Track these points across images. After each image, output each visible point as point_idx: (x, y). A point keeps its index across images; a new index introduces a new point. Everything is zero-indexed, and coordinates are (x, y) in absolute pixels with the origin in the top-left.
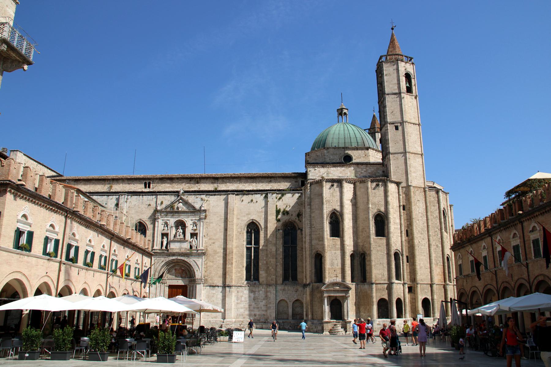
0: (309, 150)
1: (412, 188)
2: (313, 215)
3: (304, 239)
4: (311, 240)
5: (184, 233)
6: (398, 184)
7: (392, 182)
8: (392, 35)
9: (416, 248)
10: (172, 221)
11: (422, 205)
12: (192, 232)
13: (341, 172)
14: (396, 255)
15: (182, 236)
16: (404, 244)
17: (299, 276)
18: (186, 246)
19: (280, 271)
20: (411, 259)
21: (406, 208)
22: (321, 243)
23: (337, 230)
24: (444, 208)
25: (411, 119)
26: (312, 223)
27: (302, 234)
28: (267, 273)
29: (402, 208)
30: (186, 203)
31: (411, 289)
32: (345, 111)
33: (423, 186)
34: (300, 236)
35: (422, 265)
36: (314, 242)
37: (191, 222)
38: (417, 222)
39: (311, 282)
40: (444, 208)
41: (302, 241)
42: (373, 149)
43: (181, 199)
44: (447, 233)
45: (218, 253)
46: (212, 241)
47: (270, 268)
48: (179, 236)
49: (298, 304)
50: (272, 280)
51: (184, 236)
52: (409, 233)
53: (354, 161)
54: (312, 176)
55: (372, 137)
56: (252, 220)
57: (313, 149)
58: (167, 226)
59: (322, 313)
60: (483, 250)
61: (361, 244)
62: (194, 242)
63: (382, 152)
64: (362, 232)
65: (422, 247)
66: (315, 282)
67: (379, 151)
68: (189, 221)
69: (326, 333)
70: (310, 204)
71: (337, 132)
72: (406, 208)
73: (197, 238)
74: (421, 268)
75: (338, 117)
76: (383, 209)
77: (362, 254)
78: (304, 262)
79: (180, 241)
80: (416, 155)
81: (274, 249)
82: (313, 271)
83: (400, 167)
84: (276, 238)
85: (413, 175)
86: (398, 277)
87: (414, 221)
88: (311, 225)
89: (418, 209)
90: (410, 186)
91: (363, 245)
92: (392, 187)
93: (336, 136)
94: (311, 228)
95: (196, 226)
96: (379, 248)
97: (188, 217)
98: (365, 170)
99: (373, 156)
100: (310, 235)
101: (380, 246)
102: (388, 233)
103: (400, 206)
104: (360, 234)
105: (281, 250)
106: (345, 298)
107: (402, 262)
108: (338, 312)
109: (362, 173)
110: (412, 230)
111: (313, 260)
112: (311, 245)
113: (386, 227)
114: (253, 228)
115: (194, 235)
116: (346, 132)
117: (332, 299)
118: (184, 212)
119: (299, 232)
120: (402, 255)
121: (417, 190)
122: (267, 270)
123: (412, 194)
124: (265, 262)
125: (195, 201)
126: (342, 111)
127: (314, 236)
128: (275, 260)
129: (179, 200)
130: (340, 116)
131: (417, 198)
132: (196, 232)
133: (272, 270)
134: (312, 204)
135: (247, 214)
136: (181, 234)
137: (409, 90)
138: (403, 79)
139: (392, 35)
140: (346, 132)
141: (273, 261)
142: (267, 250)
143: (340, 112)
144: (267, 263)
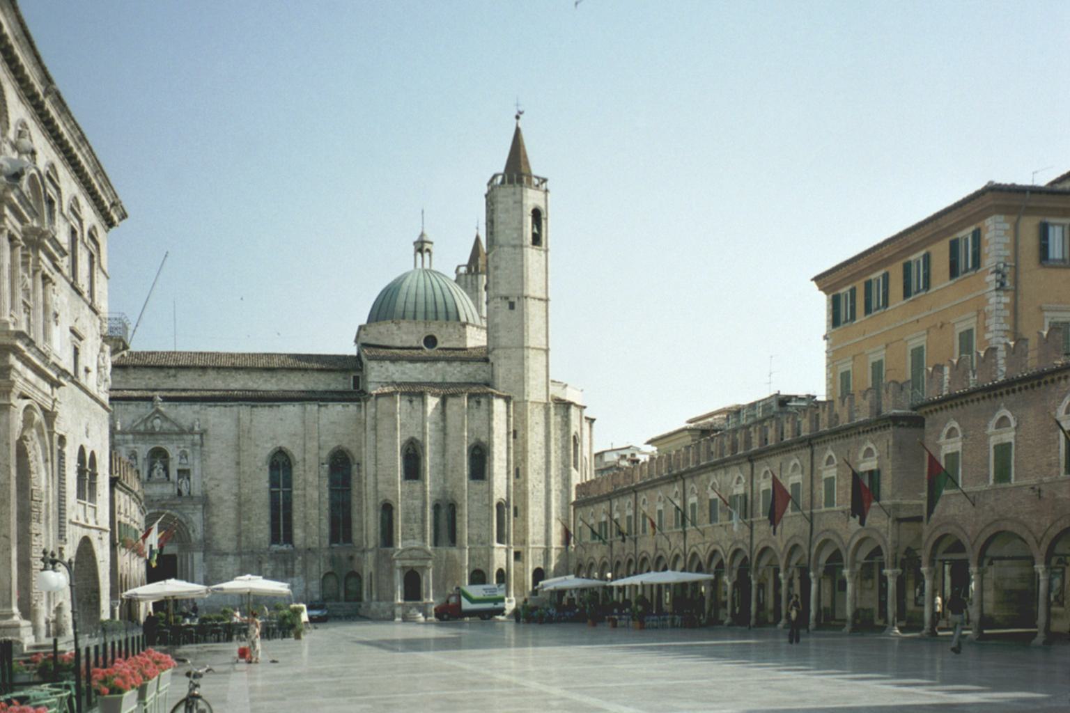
0: (364, 321)
1: (529, 404)
2: (379, 446)
3: (364, 481)
4: (376, 484)
5: (166, 469)
6: (507, 399)
7: (499, 396)
8: (518, 131)
9: (530, 494)
10: (143, 449)
11: (540, 430)
12: (181, 467)
13: (421, 372)
14: (499, 505)
15: (163, 475)
16: (512, 490)
17: (356, 536)
18: (169, 490)
19: (326, 529)
20: (520, 512)
21: (516, 434)
22: (392, 488)
23: (413, 469)
24: (576, 433)
25: (535, 291)
26: (378, 457)
27: (359, 471)
28: (305, 531)
29: (512, 435)
30: (165, 418)
31: (518, 555)
32: (427, 246)
33: (545, 401)
34: (356, 473)
35: (535, 520)
36: (380, 486)
37: (178, 452)
38: (534, 456)
39: (376, 546)
40: (576, 433)
41: (360, 482)
42: (473, 325)
43: (158, 411)
44: (577, 469)
45: (226, 501)
46: (216, 482)
47: (311, 524)
48: (159, 474)
49: (352, 580)
50: (313, 543)
51: (167, 475)
52: (518, 472)
53: (440, 345)
54: (376, 376)
55: (472, 299)
56: (280, 448)
57: (369, 321)
58: (136, 458)
59: (393, 591)
60: (599, 514)
61: (450, 490)
62: (184, 485)
63: (487, 329)
64: (452, 471)
65: (538, 494)
66: (381, 547)
67: (482, 328)
68: (173, 450)
69: (398, 619)
70: (375, 428)
71: (413, 291)
72: (516, 434)
73: (189, 479)
74: (534, 525)
75: (415, 255)
76: (483, 439)
77: (451, 505)
78: (364, 515)
79: (159, 482)
80: (539, 352)
81: (316, 495)
82: (379, 530)
83: (513, 371)
84: (319, 477)
85: (532, 382)
86: (499, 541)
87: (529, 454)
88: (376, 460)
89: (535, 437)
90: (527, 401)
91: (453, 492)
92: (499, 405)
93: (411, 299)
94: (376, 465)
95: (186, 457)
96: (475, 497)
97: (172, 441)
98: (459, 369)
99: (472, 338)
100: (376, 475)
101: (476, 494)
102: (491, 474)
103: (508, 434)
104: (449, 474)
105: (327, 495)
106: (424, 568)
107: (509, 514)
108: (413, 590)
109: (454, 374)
110: (525, 469)
111: (379, 514)
112: (377, 491)
113: (487, 465)
114: (281, 464)
115: (184, 473)
116: (430, 292)
117: (407, 570)
118: (164, 433)
119: (354, 467)
120: (508, 506)
121: (537, 407)
122: (306, 526)
123: (529, 414)
124: (302, 515)
125: (185, 414)
126: (422, 247)
127: (380, 478)
128: (317, 511)
129: (153, 414)
130: (419, 255)
131: (535, 420)
132: (186, 467)
133: (314, 527)
134: (378, 428)
135: (272, 439)
136: (161, 471)
137: (537, 240)
138: (529, 220)
139: (518, 131)
140: (430, 292)
141: (314, 513)
142: (305, 496)
143: (419, 246)
144: (305, 517)
